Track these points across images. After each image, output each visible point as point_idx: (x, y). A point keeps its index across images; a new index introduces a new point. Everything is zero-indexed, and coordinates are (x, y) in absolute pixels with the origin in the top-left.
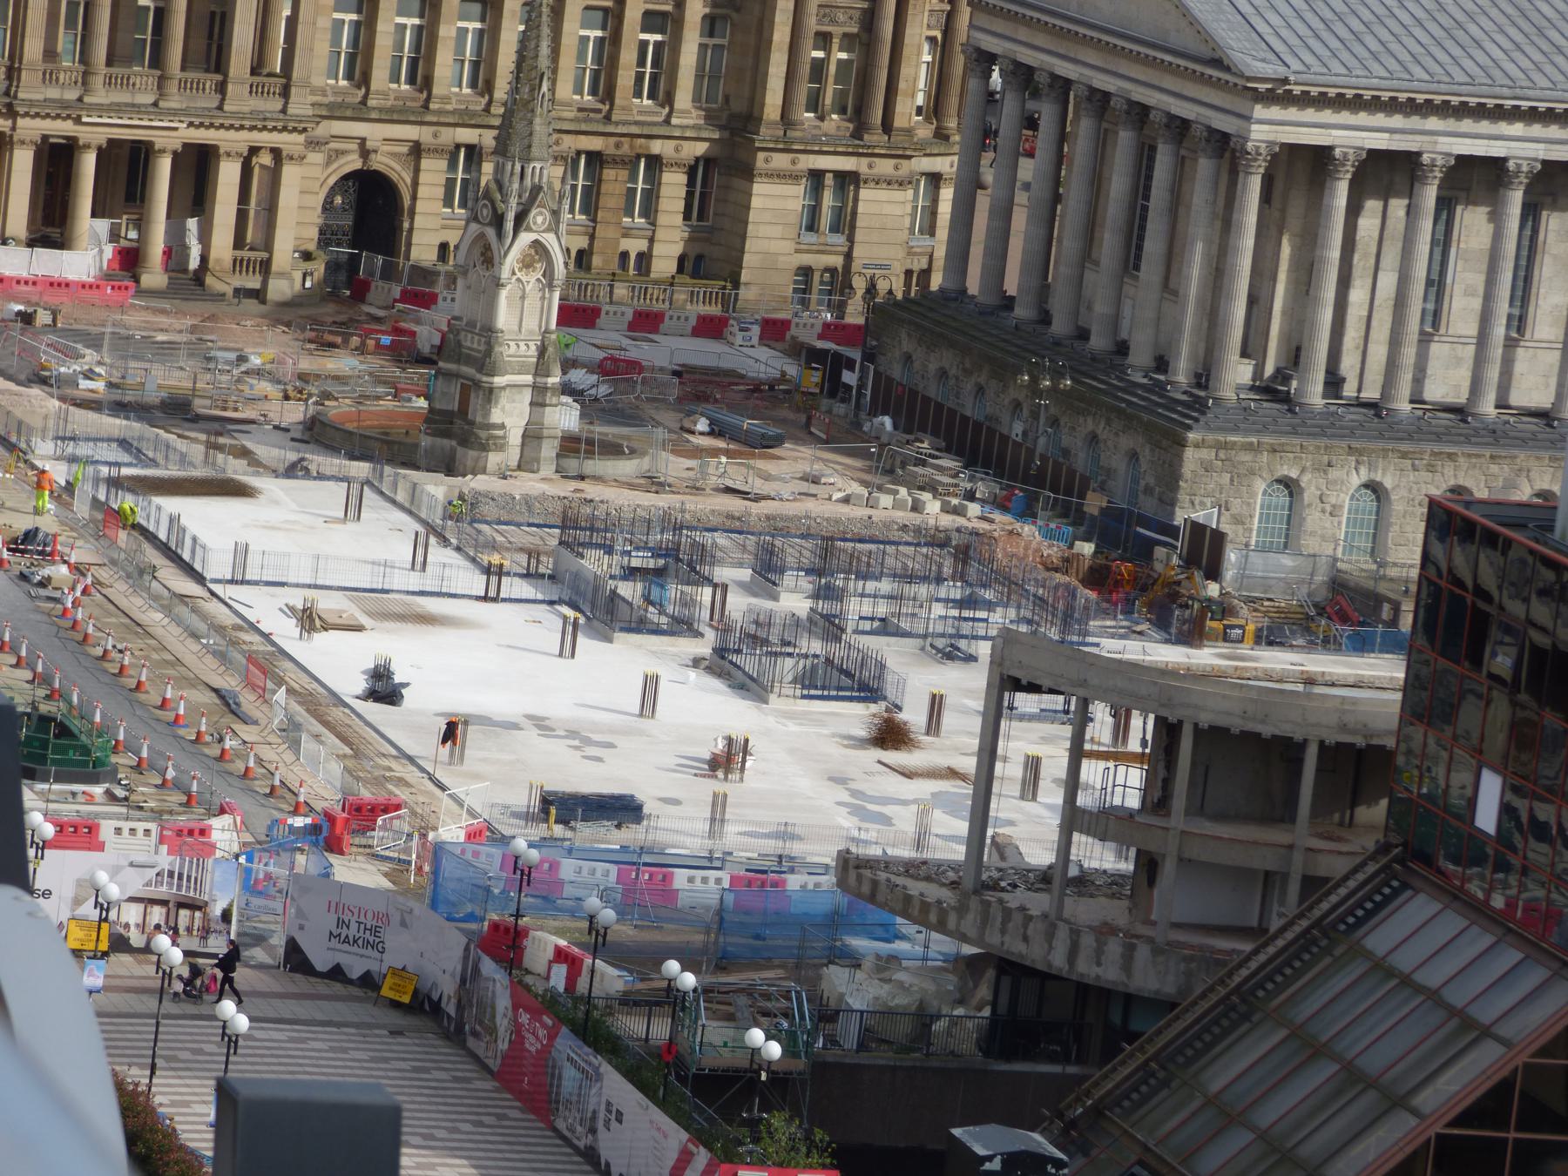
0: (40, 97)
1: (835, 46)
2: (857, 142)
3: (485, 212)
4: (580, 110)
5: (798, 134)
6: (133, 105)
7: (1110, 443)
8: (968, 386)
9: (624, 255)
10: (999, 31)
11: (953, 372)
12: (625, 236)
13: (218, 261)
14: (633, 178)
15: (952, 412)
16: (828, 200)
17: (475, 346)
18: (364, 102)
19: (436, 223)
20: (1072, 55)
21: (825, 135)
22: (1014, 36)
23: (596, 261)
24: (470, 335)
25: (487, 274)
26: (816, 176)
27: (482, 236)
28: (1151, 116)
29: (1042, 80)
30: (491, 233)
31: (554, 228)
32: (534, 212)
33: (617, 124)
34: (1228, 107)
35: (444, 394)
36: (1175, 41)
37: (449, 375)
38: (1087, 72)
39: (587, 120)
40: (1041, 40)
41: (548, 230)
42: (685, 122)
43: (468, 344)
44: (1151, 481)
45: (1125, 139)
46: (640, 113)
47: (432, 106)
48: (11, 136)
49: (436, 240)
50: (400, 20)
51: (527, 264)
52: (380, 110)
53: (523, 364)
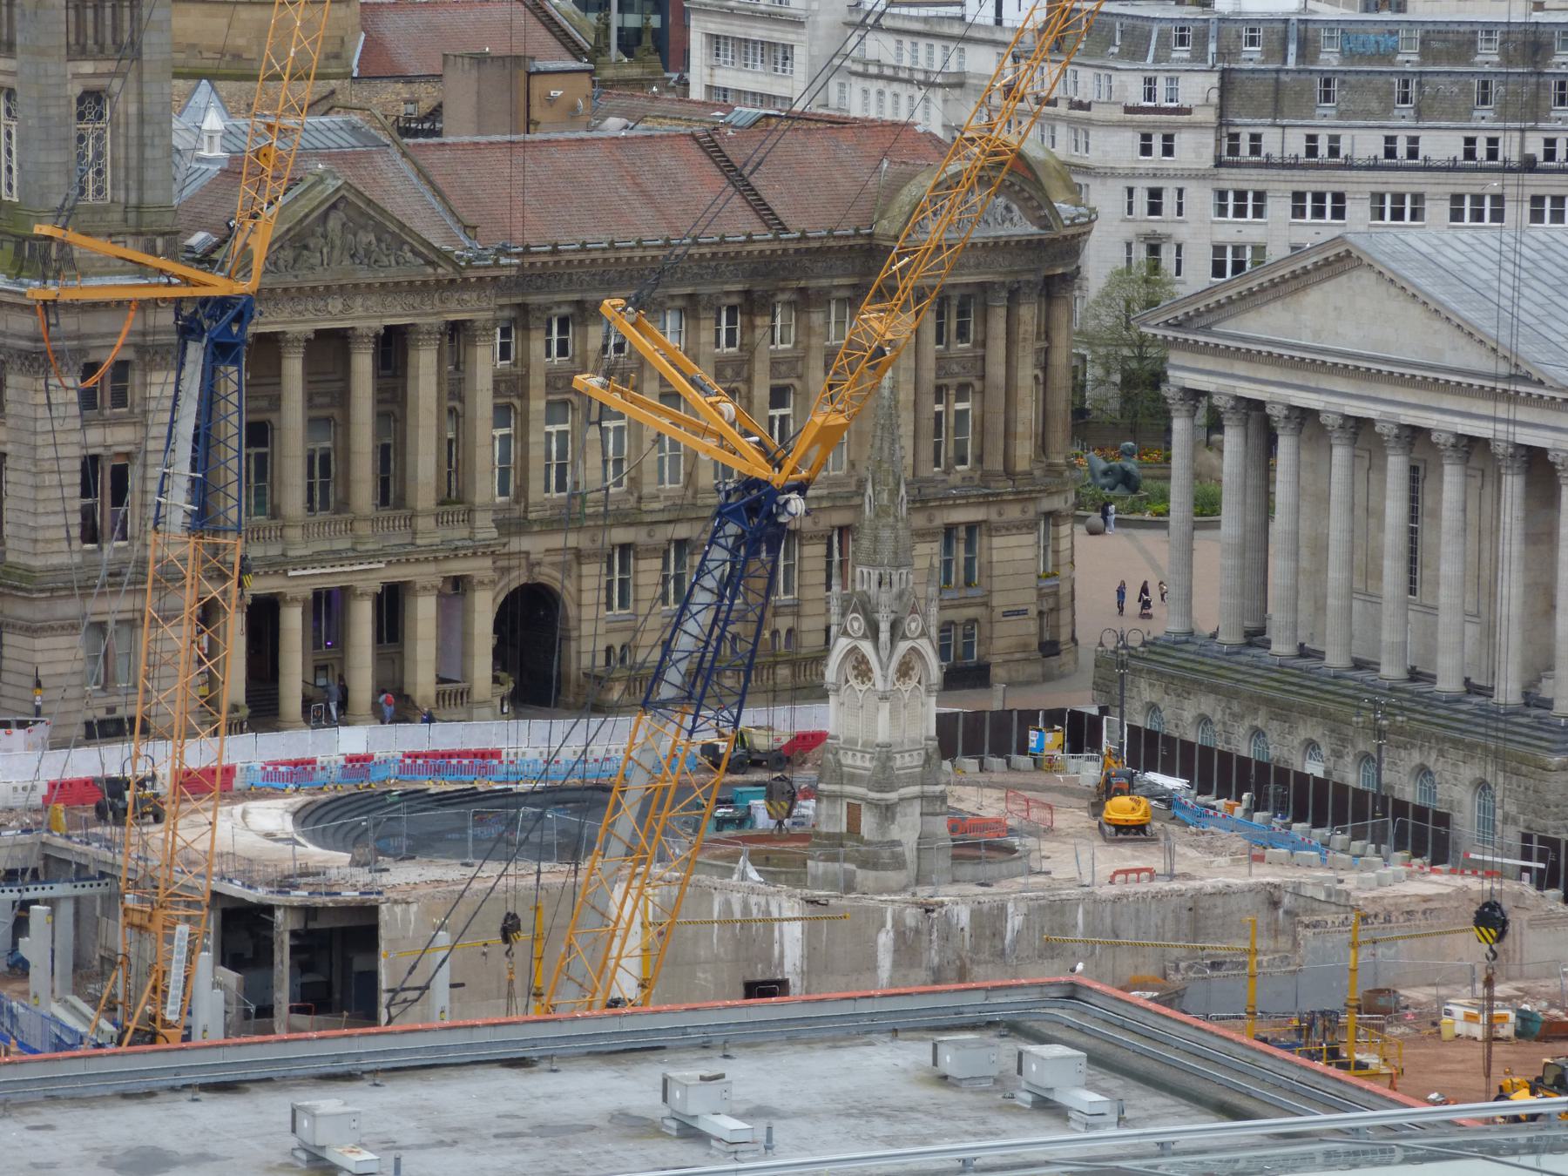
1: (952, 398)
3: (856, 625)
5: (932, 490)
6: (333, 552)
7: (1447, 775)
8: (1241, 730)
10: (1209, 367)
11: (1218, 716)
13: (425, 698)
15: (1226, 757)
16: (960, 552)
17: (859, 763)
20: (1312, 384)
21: (955, 488)
25: (864, 688)
26: (949, 531)
27: (854, 650)
28: (1433, 438)
30: (866, 647)
31: (924, 634)
34: (1537, 421)
35: (830, 817)
36: (1451, 360)
37: (834, 797)
40: (1266, 373)
41: (923, 634)
43: (850, 762)
44: (1512, 809)
45: (1396, 465)
49: (601, 645)
52: (541, 521)
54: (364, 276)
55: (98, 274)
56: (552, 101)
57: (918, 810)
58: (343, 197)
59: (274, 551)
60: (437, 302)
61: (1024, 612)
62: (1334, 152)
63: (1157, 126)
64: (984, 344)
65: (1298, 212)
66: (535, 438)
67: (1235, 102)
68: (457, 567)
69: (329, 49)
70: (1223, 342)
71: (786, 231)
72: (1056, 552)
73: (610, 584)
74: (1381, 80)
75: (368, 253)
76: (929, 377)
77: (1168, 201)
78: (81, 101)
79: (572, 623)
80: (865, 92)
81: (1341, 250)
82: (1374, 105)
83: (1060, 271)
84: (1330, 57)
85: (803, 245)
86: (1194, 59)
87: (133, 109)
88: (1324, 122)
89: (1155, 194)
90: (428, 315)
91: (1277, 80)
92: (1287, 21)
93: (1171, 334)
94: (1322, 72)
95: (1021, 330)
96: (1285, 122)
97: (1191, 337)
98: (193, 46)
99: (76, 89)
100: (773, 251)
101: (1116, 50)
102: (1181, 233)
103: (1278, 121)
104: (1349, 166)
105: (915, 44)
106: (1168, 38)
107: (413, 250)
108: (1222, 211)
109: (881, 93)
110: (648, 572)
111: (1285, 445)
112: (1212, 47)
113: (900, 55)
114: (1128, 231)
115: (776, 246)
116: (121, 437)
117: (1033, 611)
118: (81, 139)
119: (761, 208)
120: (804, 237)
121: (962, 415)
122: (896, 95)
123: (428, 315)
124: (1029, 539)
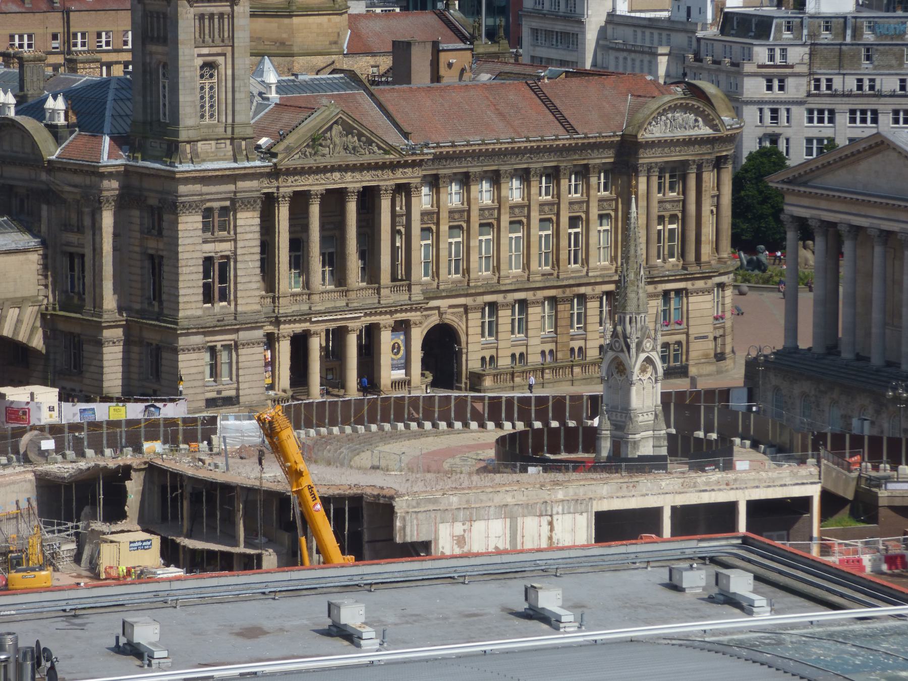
0: (290, 311)
1: (667, 222)
2: (686, 272)
4: (543, 275)
9: (572, 350)
10: (807, 204)
12: (572, 340)
13: (385, 385)
14: (572, 308)
17: (619, 419)
18: (438, 287)
19: (478, 347)
22: (817, 206)
23: (560, 355)
24: (614, 413)
26: (666, 294)
29: (843, 229)
32: (645, 342)
33: (563, 280)
38: (875, 221)
39: (548, 280)
40: (837, 207)
41: (653, 349)
42: (595, 274)
46: (573, 272)
47: (471, 284)
48: (278, 334)
50: (450, 240)
51: (643, 370)
53: (647, 426)
54: (352, 160)
55: (212, 161)
56: (450, 65)
57: (651, 444)
58: (341, 118)
59: (305, 307)
60: (391, 174)
61: (705, 337)
62: (872, 88)
63: (775, 76)
64: (684, 193)
65: (853, 120)
66: (443, 246)
67: (817, 62)
68: (400, 316)
69: (332, 39)
70: (814, 191)
71: (577, 133)
72: (723, 304)
73: (483, 323)
74: (896, 49)
75: (354, 148)
76: (655, 211)
77: (783, 115)
78: (202, 68)
79: (464, 345)
80: (617, 58)
81: (879, 140)
82: (894, 62)
83: (724, 154)
84: (869, 37)
85: (586, 141)
86: (795, 39)
87: (229, 72)
88: (866, 71)
89: (774, 112)
90: (386, 180)
91: (840, 49)
92: (845, 18)
93: (785, 187)
94: (865, 45)
95: (704, 185)
96: (845, 72)
97: (796, 188)
98: (259, 39)
99: (199, 62)
100: (570, 144)
101: (752, 34)
102: (788, 132)
103: (842, 72)
104: (880, 95)
105: (643, 33)
106: (781, 27)
107: (378, 146)
108: (811, 120)
109: (625, 59)
110: (505, 316)
111: (847, 247)
112: (805, 32)
113: (635, 39)
114: (760, 132)
115: (572, 142)
116: (225, 248)
117: (711, 337)
118: (202, 88)
119: (564, 122)
120: (586, 137)
121: (672, 231)
122: (633, 60)
123: (386, 180)
124: (709, 297)
